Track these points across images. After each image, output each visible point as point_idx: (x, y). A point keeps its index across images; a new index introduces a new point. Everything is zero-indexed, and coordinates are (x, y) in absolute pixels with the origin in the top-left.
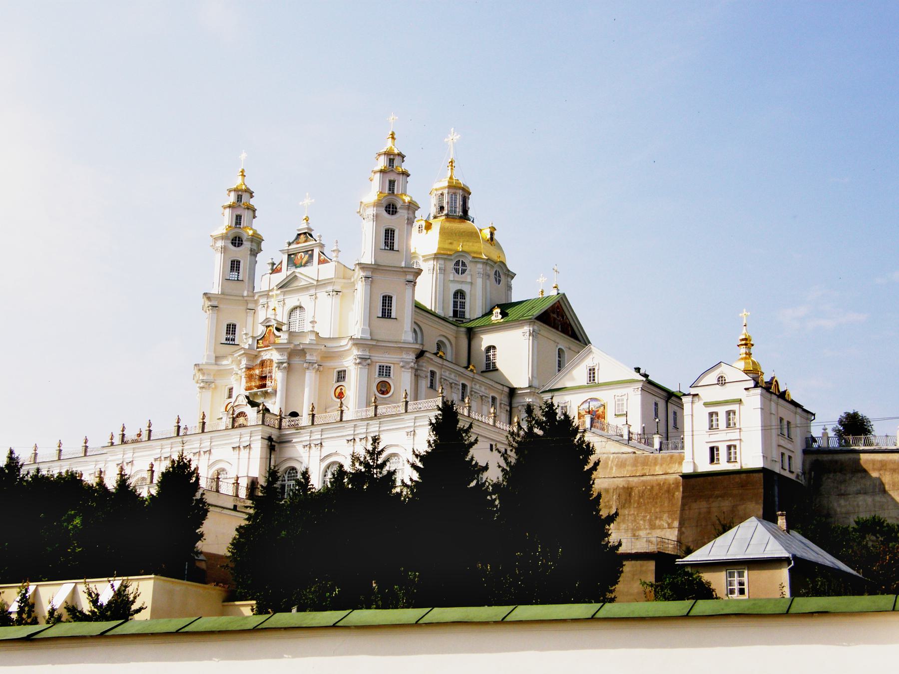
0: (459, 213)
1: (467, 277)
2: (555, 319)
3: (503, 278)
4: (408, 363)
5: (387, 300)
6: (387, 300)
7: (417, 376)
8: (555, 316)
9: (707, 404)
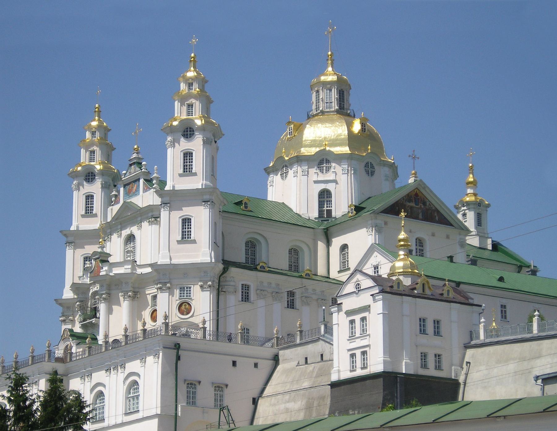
1: (330, 176)
5: (186, 222)
6: (186, 222)
8: (412, 204)
9: (349, 313)
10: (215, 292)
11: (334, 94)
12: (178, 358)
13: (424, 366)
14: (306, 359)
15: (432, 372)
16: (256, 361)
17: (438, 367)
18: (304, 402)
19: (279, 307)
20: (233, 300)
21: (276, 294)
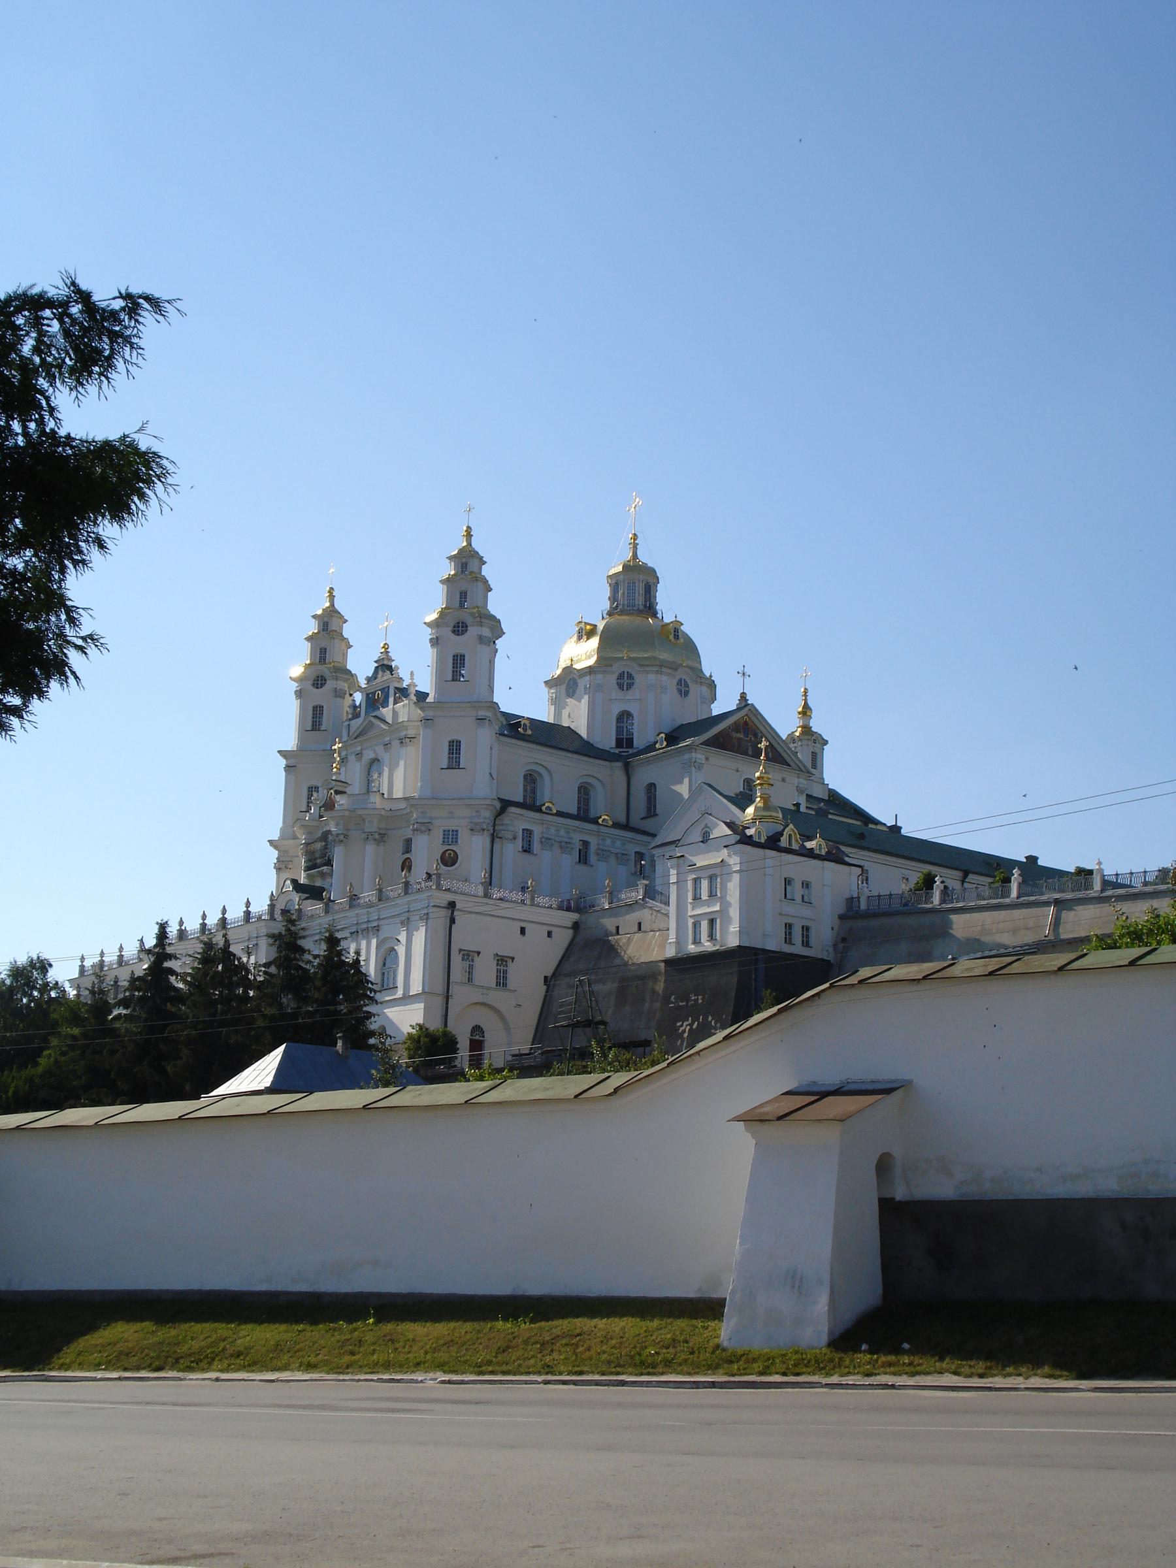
0: (640, 601)
1: (630, 695)
2: (740, 739)
3: (693, 688)
4: (476, 824)
5: (455, 748)
6: (455, 748)
7: (494, 837)
8: (740, 735)
10: (488, 840)
11: (640, 589)
12: (452, 921)
13: (788, 940)
14: (618, 928)
15: (797, 949)
16: (550, 929)
17: (806, 943)
18: (616, 985)
19: (569, 860)
20: (510, 851)
21: (565, 846)
